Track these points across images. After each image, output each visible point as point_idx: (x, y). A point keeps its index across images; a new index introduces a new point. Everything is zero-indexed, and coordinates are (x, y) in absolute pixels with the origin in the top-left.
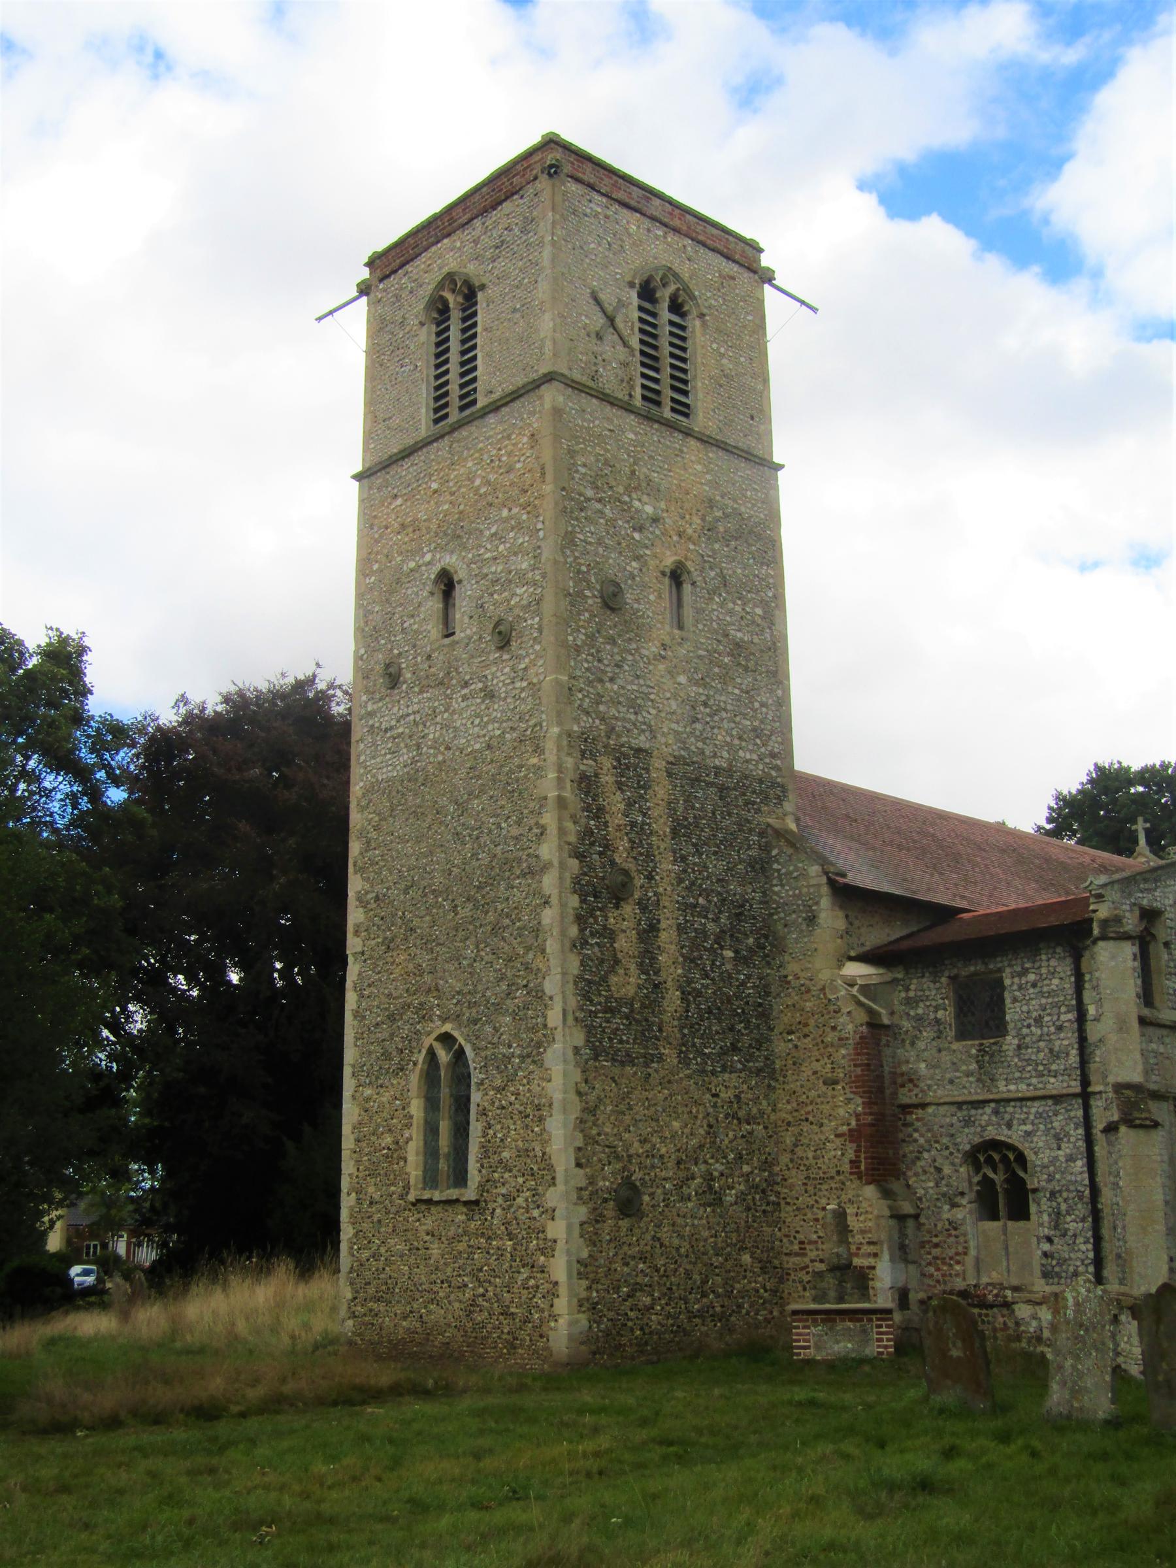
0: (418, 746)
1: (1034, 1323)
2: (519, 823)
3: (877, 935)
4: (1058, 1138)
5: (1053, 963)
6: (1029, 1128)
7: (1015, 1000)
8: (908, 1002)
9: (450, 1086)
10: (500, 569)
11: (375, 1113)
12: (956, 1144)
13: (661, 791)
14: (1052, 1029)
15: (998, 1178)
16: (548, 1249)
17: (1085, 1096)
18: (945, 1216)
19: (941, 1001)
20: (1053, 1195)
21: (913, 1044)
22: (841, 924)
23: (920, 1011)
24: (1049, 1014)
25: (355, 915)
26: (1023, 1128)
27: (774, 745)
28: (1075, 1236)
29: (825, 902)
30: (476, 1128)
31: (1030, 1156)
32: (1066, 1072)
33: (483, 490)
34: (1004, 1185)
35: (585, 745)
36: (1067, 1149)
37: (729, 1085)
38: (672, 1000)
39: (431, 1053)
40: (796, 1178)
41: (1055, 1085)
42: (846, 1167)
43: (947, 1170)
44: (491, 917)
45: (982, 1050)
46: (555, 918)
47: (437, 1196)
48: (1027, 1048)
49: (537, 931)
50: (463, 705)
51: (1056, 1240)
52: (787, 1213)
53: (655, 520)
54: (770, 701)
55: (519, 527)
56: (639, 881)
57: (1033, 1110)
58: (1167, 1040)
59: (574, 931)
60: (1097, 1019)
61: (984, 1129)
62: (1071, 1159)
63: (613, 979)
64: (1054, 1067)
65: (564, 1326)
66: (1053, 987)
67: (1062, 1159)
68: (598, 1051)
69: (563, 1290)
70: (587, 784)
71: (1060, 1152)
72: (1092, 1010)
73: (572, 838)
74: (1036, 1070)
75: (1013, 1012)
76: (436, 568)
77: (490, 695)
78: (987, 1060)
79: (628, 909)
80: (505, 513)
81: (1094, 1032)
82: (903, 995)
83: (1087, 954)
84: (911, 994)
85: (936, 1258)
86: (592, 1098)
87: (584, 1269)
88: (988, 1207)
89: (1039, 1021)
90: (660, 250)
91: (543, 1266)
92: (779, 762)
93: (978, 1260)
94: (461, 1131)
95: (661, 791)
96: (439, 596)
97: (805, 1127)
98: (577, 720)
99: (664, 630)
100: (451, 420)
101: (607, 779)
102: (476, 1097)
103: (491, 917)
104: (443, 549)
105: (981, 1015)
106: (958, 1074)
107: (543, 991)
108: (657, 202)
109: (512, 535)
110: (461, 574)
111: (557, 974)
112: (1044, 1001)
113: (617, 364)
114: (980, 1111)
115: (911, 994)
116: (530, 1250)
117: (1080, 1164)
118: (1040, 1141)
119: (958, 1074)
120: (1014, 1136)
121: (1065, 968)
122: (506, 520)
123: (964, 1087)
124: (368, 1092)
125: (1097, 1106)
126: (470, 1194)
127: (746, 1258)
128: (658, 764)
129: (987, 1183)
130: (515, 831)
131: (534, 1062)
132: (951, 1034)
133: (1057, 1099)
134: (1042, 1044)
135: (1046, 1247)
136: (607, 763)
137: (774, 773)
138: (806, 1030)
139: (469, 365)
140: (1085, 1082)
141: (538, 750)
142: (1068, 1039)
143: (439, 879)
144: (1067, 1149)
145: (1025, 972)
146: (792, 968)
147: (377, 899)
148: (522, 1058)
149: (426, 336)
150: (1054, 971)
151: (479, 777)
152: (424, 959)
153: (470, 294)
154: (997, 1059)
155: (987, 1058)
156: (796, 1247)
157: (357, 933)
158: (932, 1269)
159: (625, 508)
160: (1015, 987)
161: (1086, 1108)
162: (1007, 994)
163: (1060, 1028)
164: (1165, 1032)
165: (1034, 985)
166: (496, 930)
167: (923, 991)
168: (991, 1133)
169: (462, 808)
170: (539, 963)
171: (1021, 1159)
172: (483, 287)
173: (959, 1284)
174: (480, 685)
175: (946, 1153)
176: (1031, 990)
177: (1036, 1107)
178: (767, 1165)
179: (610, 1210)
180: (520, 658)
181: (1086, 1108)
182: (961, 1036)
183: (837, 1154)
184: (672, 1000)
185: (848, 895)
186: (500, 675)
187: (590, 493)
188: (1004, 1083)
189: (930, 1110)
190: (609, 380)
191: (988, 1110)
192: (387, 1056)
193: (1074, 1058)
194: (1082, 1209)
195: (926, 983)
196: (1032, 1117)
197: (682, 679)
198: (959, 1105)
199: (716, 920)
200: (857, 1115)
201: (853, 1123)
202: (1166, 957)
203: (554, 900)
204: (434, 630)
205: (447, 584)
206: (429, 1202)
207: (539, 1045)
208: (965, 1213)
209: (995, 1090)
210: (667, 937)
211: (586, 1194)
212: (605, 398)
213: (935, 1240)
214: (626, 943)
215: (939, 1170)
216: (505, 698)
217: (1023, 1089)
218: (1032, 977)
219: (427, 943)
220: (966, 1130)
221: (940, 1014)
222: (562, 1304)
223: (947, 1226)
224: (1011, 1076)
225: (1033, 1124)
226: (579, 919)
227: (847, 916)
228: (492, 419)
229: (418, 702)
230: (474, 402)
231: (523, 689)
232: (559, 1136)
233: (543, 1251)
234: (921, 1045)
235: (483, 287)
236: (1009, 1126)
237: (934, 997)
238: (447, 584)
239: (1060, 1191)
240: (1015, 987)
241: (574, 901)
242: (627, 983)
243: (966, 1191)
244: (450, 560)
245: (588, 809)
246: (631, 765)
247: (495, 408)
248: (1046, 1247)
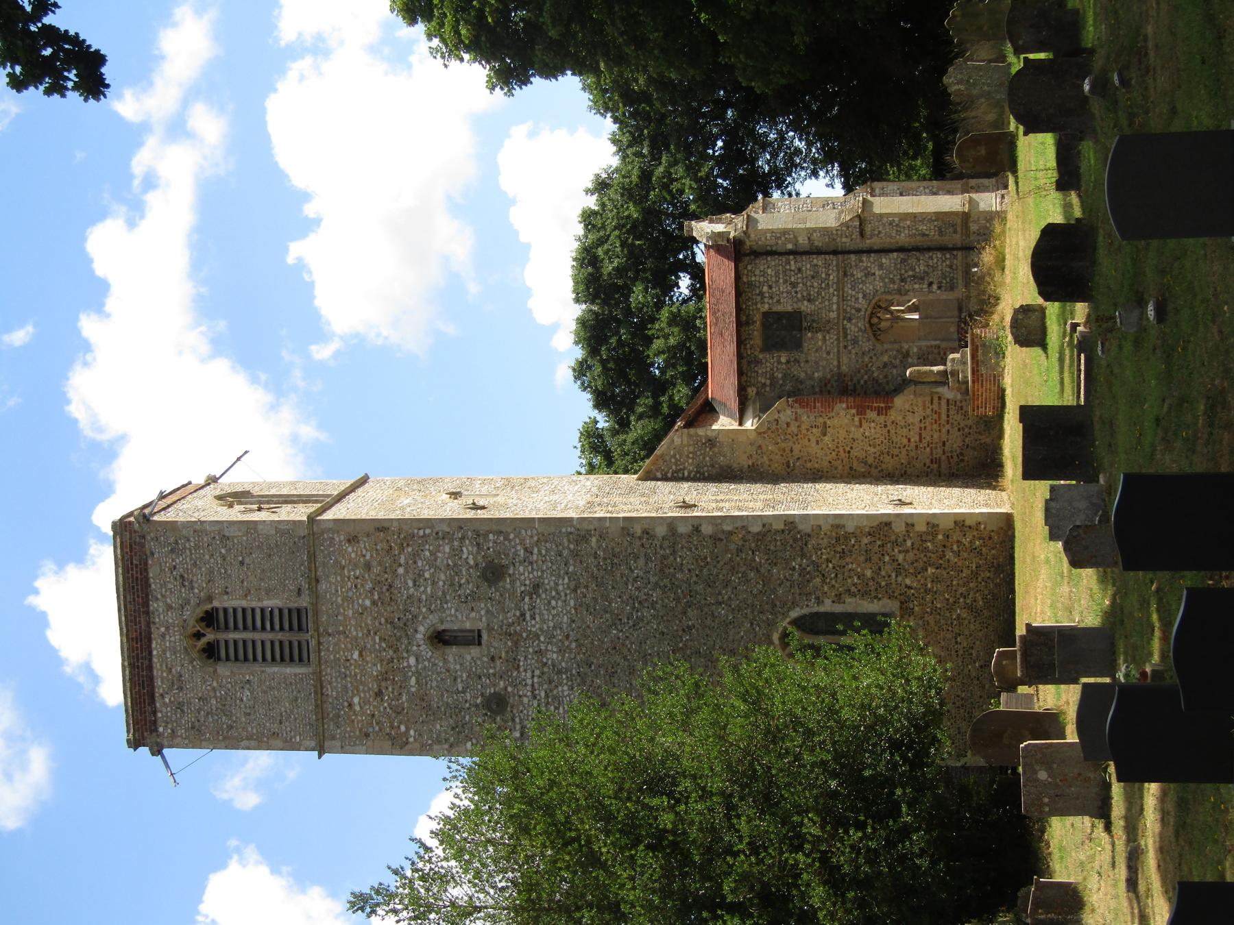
2: (636, 558)
6: (861, 295)
7: (778, 301)
10: (443, 577)
20: (902, 280)
21: (801, 382)
23: (780, 376)
29: (701, 431)
43: (885, 359)
50: (538, 618)
61: (860, 330)
72: (790, 246)
75: (787, 306)
76: (426, 651)
84: (768, 382)
89: (794, 285)
93: (944, 340)
107: (758, 534)
121: (761, 264)
130: (642, 562)
132: (796, 354)
135: (935, 287)
142: (807, 264)
145: (761, 294)
151: (595, 600)
155: (815, 325)
162: (774, 309)
163: (800, 270)
174: (527, 599)
182: (798, 345)
186: (523, 575)
193: (819, 261)
201: (854, 411)
205: (440, 639)
215: (885, 365)
218: (765, 289)
221: (783, 360)
236: (859, 310)
238: (440, 639)
248: (935, 287)
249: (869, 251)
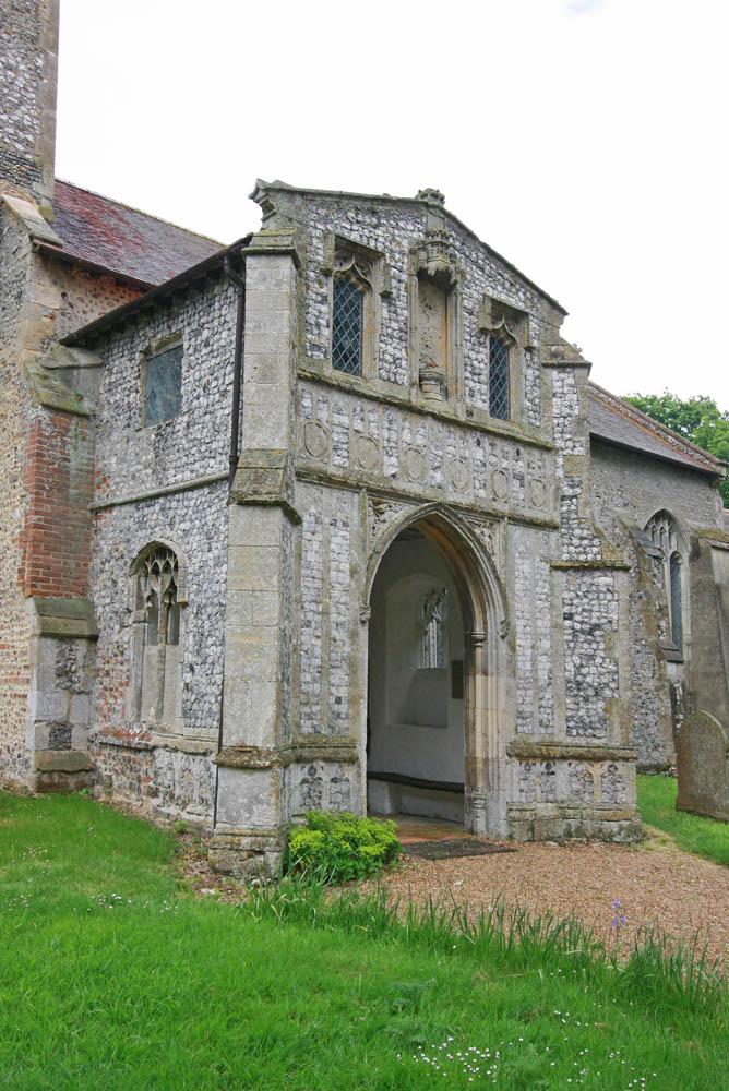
6: (186, 525)
7: (190, 367)
12: (129, 551)
14: (217, 397)
18: (116, 638)
19: (134, 382)
24: (216, 379)
26: (183, 526)
27: (24, 115)
28: (213, 664)
48: (195, 424)
51: (197, 668)
54: (22, 67)
57: (192, 503)
58: (372, 417)
64: (214, 446)
66: (223, 342)
67: (211, 563)
71: (210, 555)
74: (199, 451)
82: (107, 381)
85: (105, 689)
92: (30, 138)
106: (139, 467)
112: (213, 361)
114: (152, 509)
118: (195, 540)
119: (139, 467)
123: (143, 482)
133: (210, 484)
137: (20, 147)
154: (168, 444)
158: (102, 702)
160: (191, 351)
164: (369, 406)
167: (121, 372)
176: (205, 351)
188: (173, 472)
191: (157, 507)
196: (190, 512)
202: (385, 313)
209: (165, 482)
213: (107, 667)
220: (139, 534)
223: (116, 651)
224: (178, 464)
225: (191, 521)
227: (64, 295)
236: (171, 524)
239: (205, 606)
240: (191, 351)
243: (133, 607)
248: (188, 677)
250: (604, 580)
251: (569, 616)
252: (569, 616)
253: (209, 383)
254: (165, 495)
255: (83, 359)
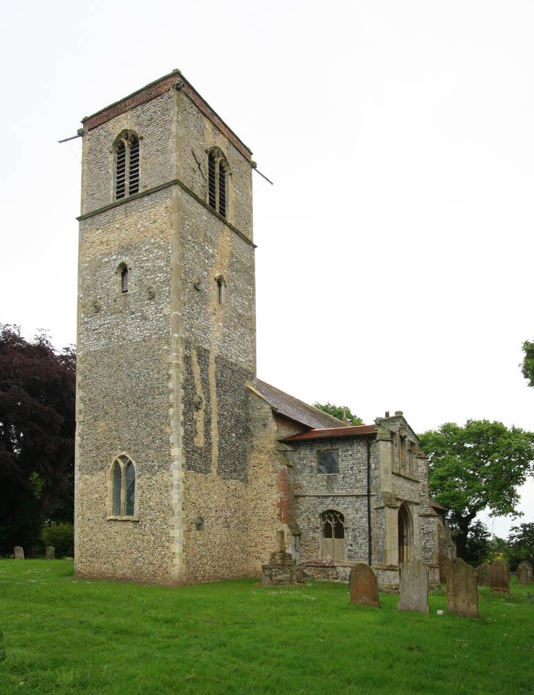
0: (110, 338)
1: (344, 573)
3: (286, 433)
4: (356, 510)
5: (359, 448)
6: (346, 506)
7: (343, 461)
8: (300, 459)
9: (124, 478)
11: (90, 487)
13: (212, 368)
15: (333, 523)
16: (171, 540)
17: (369, 496)
18: (311, 535)
20: (354, 530)
22: (275, 428)
25: (79, 406)
30: (137, 492)
31: (345, 515)
32: (361, 487)
33: (142, 230)
34: (334, 525)
35: (187, 344)
36: (360, 514)
37: (233, 483)
38: (215, 451)
39: (116, 463)
40: (255, 519)
41: (357, 492)
42: (276, 517)
43: (312, 520)
44: (145, 410)
45: (328, 477)
46: (176, 412)
47: (118, 518)
49: (166, 417)
50: (132, 322)
52: (251, 532)
53: (213, 256)
55: (160, 247)
56: (204, 402)
59: (182, 418)
60: (375, 469)
61: (328, 505)
62: (361, 518)
63: (195, 439)
65: (177, 567)
68: (189, 466)
69: (177, 556)
70: (187, 359)
72: (373, 466)
73: (182, 381)
75: (341, 465)
76: (119, 262)
77: (145, 318)
78: (330, 481)
79: (201, 412)
80: (153, 241)
81: (374, 473)
83: (373, 446)
84: (301, 456)
86: (188, 483)
87: (185, 548)
88: (327, 533)
89: (352, 468)
90: (221, 143)
91: (168, 547)
94: (130, 492)
95: (212, 368)
96: (120, 274)
97: (259, 501)
98: (184, 333)
99: (214, 303)
100: (126, 197)
101: (195, 359)
102: (137, 481)
103: (145, 410)
104: (122, 254)
105: (329, 465)
107: (169, 441)
108: (216, 118)
109: (156, 250)
110: (130, 264)
111: (175, 433)
113: (200, 184)
115: (301, 456)
116: (163, 539)
117: (365, 520)
120: (339, 509)
122: (153, 244)
124: (87, 477)
125: (373, 499)
126: (135, 517)
127: (237, 547)
128: (212, 357)
129: (327, 525)
130: (156, 376)
131: (165, 469)
133: (357, 496)
134: (353, 477)
135: (350, 548)
136: (194, 353)
138: (261, 466)
139: (134, 174)
140: (369, 491)
141: (168, 343)
142: (364, 475)
143: (120, 394)
144: (360, 514)
145: (348, 450)
146: (256, 442)
147: (90, 399)
148: (159, 467)
149: (112, 158)
150: (359, 451)
151: (139, 353)
152: (112, 425)
153: (135, 141)
156: (254, 544)
157: (80, 413)
159: (202, 248)
161: (369, 500)
163: (360, 472)
165: (351, 456)
166: (147, 415)
168: (331, 507)
169: (131, 365)
170: (168, 430)
171: (342, 517)
172: (142, 138)
173: (314, 559)
174: (140, 314)
175: (312, 514)
177: (348, 499)
178: (244, 514)
179: (194, 528)
180: (160, 304)
181: (369, 500)
183: (272, 512)
184: (215, 451)
185: (280, 418)
187: (190, 238)
189: (307, 498)
190: (197, 191)
191: (330, 499)
192: (95, 463)
193: (365, 482)
194: (364, 535)
195: (308, 452)
197: (221, 324)
198: (319, 497)
199: (230, 422)
200: (281, 499)
201: (279, 501)
203: (174, 405)
204: (118, 289)
205: (124, 270)
206: (116, 520)
207: (167, 462)
208: (319, 535)
210: (214, 425)
211: (184, 521)
212: (196, 198)
214: (200, 426)
215: (309, 519)
216: (152, 321)
217: (344, 493)
218: (350, 453)
219: (114, 419)
221: (312, 464)
222: (177, 561)
226: (184, 414)
228: (146, 199)
229: (109, 320)
230: (137, 191)
231: (160, 317)
232: (175, 497)
233: (168, 541)
234: (304, 474)
235: (142, 138)
236: (338, 505)
237: (308, 457)
238: (124, 270)
241: (182, 406)
242: (200, 441)
244: (126, 259)
245: (187, 370)
246: (203, 355)
247: (148, 193)
248: (350, 548)
249: (369, 511)
250: (432, 519)
251: (423, 529)
252: (423, 529)
253: (353, 467)
254: (334, 496)
255: (289, 448)
